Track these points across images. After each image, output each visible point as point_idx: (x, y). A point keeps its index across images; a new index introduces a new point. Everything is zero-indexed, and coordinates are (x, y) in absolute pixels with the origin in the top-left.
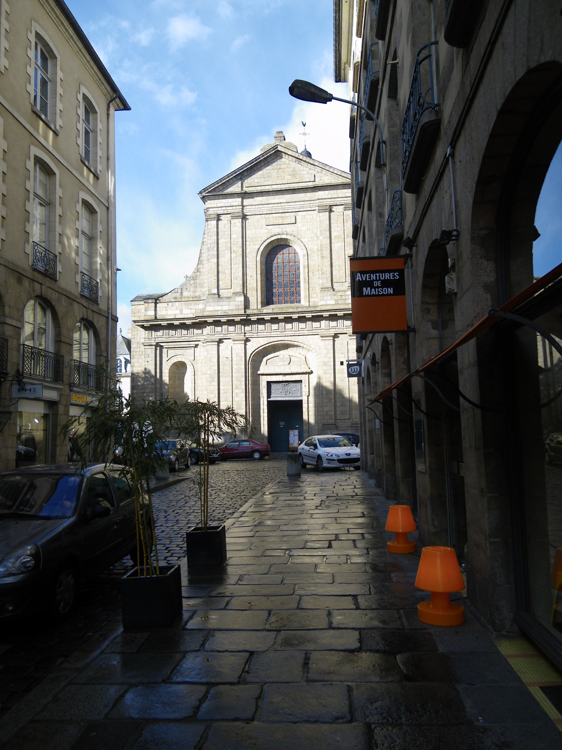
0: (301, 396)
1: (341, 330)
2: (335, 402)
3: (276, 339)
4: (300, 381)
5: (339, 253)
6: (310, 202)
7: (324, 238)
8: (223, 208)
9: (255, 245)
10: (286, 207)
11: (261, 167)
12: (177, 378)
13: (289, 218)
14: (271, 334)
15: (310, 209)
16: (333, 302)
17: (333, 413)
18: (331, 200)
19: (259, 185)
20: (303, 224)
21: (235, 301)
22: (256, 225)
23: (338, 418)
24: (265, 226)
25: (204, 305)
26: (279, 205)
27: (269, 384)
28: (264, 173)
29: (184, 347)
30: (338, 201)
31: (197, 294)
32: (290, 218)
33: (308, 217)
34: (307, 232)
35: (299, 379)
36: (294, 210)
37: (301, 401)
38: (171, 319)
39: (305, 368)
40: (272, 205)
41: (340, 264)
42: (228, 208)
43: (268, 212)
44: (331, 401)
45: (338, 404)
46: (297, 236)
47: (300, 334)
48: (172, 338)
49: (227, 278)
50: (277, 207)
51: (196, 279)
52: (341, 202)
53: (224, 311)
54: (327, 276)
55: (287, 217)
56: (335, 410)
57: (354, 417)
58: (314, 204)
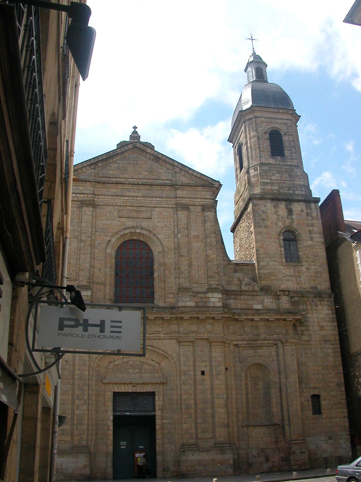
0: (154, 410)
2: (196, 418)
4: (153, 394)
6: (168, 199)
7: (182, 236)
9: (106, 236)
13: (144, 212)
15: (167, 206)
16: (192, 304)
17: (193, 431)
18: (189, 200)
19: (114, 176)
20: (159, 220)
22: (108, 216)
23: (199, 437)
24: (117, 218)
26: (135, 198)
27: (115, 394)
28: (120, 166)
33: (165, 214)
34: (163, 229)
35: (152, 391)
36: (151, 205)
37: (153, 418)
40: (127, 198)
41: (200, 264)
42: (78, 195)
43: (122, 204)
45: (200, 420)
46: (153, 232)
47: (155, 338)
52: (200, 202)
55: (142, 211)
56: (196, 427)
58: (171, 202)
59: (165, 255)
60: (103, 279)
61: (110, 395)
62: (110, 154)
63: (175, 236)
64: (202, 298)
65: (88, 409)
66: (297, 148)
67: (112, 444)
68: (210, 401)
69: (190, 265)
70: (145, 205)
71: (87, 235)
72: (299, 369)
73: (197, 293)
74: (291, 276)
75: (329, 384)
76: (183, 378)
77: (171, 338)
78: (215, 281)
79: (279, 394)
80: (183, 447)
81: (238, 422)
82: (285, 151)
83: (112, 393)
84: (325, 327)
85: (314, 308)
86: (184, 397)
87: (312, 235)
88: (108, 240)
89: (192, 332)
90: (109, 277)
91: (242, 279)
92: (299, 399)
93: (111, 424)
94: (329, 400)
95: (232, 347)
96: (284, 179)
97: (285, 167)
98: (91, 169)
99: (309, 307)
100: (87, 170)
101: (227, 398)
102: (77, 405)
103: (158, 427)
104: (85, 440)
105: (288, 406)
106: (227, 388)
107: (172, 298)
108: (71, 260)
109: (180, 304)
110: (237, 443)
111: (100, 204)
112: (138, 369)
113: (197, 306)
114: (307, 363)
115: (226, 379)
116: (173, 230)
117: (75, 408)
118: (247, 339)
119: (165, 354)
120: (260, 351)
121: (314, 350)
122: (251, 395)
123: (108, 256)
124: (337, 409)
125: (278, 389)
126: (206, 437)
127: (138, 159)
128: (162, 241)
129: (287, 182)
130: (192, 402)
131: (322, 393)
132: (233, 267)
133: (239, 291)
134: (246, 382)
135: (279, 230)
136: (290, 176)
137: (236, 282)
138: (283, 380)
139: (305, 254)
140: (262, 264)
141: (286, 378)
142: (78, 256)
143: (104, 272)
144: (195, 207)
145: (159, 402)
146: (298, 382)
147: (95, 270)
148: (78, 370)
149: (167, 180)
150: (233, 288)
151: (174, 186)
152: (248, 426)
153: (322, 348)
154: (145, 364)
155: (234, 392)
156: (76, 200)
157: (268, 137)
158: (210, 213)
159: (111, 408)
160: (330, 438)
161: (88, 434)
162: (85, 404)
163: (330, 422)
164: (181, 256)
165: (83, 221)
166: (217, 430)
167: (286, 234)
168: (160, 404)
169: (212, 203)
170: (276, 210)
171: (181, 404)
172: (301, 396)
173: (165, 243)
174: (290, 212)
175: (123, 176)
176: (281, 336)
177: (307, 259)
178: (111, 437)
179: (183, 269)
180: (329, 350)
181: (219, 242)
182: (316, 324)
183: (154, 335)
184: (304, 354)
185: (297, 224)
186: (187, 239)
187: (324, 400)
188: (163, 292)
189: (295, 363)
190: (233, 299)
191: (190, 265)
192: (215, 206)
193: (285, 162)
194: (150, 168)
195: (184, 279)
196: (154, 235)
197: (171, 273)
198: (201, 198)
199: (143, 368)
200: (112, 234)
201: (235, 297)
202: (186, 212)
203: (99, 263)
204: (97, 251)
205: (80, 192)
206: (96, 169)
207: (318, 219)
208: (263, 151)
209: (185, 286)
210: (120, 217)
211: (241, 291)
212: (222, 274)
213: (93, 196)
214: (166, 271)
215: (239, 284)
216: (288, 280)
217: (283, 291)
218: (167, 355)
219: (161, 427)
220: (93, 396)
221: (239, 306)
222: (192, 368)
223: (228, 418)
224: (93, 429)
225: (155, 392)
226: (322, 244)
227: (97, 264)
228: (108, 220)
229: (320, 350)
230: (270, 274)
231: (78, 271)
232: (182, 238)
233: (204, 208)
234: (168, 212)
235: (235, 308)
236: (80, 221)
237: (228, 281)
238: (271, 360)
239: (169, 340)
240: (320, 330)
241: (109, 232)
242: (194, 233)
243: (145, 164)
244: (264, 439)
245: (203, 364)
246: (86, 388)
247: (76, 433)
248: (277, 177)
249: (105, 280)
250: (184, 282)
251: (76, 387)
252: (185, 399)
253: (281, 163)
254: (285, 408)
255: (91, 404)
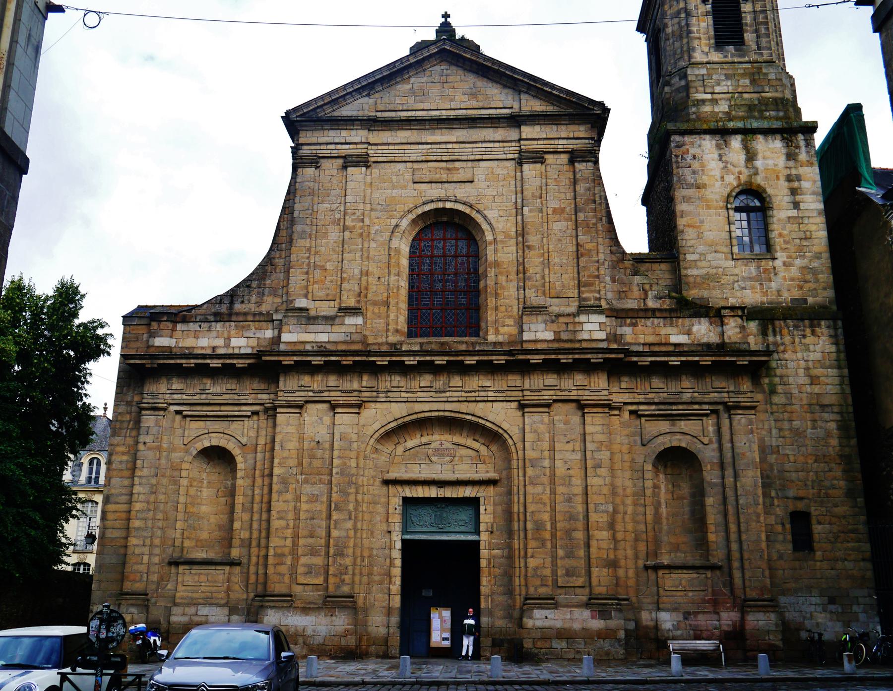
0: (478, 532)
1: (566, 393)
2: (554, 547)
3: (427, 407)
4: (474, 503)
5: (561, 240)
6: (505, 144)
7: (530, 211)
8: (330, 147)
9: (391, 217)
10: (455, 150)
11: (409, 77)
12: (205, 482)
13: (461, 171)
14: (416, 395)
15: (504, 157)
16: (550, 336)
17: (548, 572)
18: (545, 142)
19: (405, 108)
20: (488, 183)
21: (343, 324)
23: (560, 584)
24: (411, 184)
25: (276, 332)
26: (444, 146)
27: (408, 502)
28: (415, 88)
29: (227, 416)
30: (561, 145)
31: (264, 308)
32: (463, 171)
35: (473, 495)
36: (472, 157)
38: (204, 356)
39: (487, 472)
40: (429, 146)
41: (564, 261)
42: (339, 147)
43: (420, 159)
44: (544, 545)
45: (561, 553)
47: (478, 399)
48: (204, 396)
49: (329, 278)
50: (439, 151)
51: (264, 279)
52: (565, 146)
53: (319, 345)
54: (537, 283)
55: (458, 169)
56: (554, 565)
57: (595, 581)
59: (500, 247)
60: (386, 294)
61: (396, 502)
62: (395, 67)
63: (519, 210)
64: (567, 324)
65: (355, 529)
66: (771, 26)
67: (400, 593)
68: (581, 517)
69: (547, 264)
70: (463, 158)
71: (356, 216)
72: (763, 460)
73: (558, 316)
74: (751, 279)
75: (830, 491)
76: (530, 472)
77: (507, 399)
78: (592, 291)
79: (722, 507)
80: (528, 601)
81: (636, 557)
82: (745, 35)
83: (401, 498)
84: (821, 378)
85: (797, 340)
86: (531, 508)
87: (797, 197)
88: (394, 224)
89: (547, 388)
90: (395, 291)
91: (647, 287)
92: (762, 519)
93: (397, 555)
94: (830, 524)
95: (626, 415)
96: (740, 90)
97: (745, 66)
98: (362, 97)
99: (787, 339)
100: (355, 100)
101: (615, 511)
102: (336, 521)
103: (483, 563)
104: (348, 584)
105: (739, 532)
106: (614, 493)
107: (511, 326)
108: (328, 264)
109: (526, 336)
110: (634, 599)
111: (380, 159)
112: (447, 456)
113: (557, 340)
114: (780, 447)
115: (613, 476)
116: (514, 200)
117: (332, 527)
118: (656, 400)
119: (496, 428)
120: (683, 423)
121: (796, 423)
122: (666, 507)
123: (392, 254)
124: (848, 542)
125: (720, 497)
126: (572, 585)
127: (449, 71)
128: (493, 222)
129: (745, 96)
130: (546, 517)
131: (813, 508)
132: (630, 266)
133: (642, 310)
134: (654, 483)
135: (728, 190)
136: (753, 82)
137: (636, 293)
138: (729, 480)
139: (780, 235)
140: (691, 259)
141: (736, 476)
142: (340, 256)
143: (386, 283)
144: (556, 156)
145: (486, 517)
146: (760, 484)
147: (370, 279)
148: (339, 457)
149: (505, 108)
150: (631, 304)
151: (515, 120)
152: (656, 568)
153: (814, 421)
154: (460, 447)
155: (629, 501)
156: (336, 155)
157: (710, 10)
158: (584, 164)
159: (397, 527)
160: (832, 601)
161: (354, 574)
162: (350, 518)
163: (832, 569)
164: (529, 247)
165: (348, 192)
166: (595, 571)
167: (742, 197)
168: (489, 521)
169: (589, 146)
170: (721, 152)
171: (525, 521)
172: (767, 513)
173: (499, 226)
174: (751, 156)
175: (421, 106)
176: (725, 395)
177: (784, 246)
178: (398, 581)
179: (531, 271)
180: (829, 424)
181: (604, 218)
182: (801, 372)
183: (477, 394)
184: (774, 431)
185: (766, 177)
186: (540, 215)
187: (819, 523)
188: (494, 315)
189: (755, 447)
190: (629, 325)
191: (547, 264)
192: (595, 150)
193: (743, 56)
194: (471, 88)
195: (533, 291)
196: (478, 211)
197: (511, 281)
198: (567, 139)
199: (457, 454)
200: (402, 213)
201: (634, 321)
202: (538, 165)
203: (377, 267)
204: (373, 245)
205: (343, 141)
206: (372, 97)
207: (811, 164)
208: (700, 38)
209: (535, 304)
210: (415, 183)
211: (647, 310)
212: (608, 279)
213: (366, 146)
214: (500, 277)
215: (643, 297)
216: (744, 288)
217: (732, 308)
218: (501, 431)
219: (490, 563)
220: (365, 505)
221: (642, 339)
222: (546, 453)
223: (615, 549)
224: (363, 564)
225: (479, 498)
226: (819, 214)
227: (373, 267)
228: (394, 188)
229: (809, 423)
230: (708, 277)
231: (339, 283)
232: (531, 214)
233: (574, 157)
234: (505, 168)
235: (633, 341)
236: (344, 192)
237: (620, 292)
238: (706, 440)
239: (505, 403)
240: (811, 384)
241: (396, 210)
242: (553, 204)
243: (461, 81)
244: (690, 594)
245: (570, 446)
246: (352, 490)
247: (332, 570)
248: (726, 87)
249: (388, 297)
250: (535, 295)
251: (335, 489)
252: (532, 512)
253: (736, 60)
254: (733, 536)
255: (360, 518)
